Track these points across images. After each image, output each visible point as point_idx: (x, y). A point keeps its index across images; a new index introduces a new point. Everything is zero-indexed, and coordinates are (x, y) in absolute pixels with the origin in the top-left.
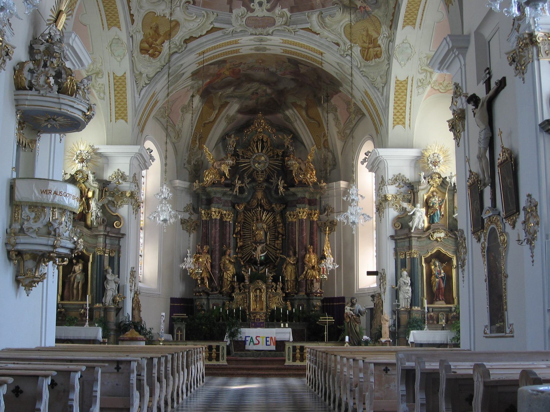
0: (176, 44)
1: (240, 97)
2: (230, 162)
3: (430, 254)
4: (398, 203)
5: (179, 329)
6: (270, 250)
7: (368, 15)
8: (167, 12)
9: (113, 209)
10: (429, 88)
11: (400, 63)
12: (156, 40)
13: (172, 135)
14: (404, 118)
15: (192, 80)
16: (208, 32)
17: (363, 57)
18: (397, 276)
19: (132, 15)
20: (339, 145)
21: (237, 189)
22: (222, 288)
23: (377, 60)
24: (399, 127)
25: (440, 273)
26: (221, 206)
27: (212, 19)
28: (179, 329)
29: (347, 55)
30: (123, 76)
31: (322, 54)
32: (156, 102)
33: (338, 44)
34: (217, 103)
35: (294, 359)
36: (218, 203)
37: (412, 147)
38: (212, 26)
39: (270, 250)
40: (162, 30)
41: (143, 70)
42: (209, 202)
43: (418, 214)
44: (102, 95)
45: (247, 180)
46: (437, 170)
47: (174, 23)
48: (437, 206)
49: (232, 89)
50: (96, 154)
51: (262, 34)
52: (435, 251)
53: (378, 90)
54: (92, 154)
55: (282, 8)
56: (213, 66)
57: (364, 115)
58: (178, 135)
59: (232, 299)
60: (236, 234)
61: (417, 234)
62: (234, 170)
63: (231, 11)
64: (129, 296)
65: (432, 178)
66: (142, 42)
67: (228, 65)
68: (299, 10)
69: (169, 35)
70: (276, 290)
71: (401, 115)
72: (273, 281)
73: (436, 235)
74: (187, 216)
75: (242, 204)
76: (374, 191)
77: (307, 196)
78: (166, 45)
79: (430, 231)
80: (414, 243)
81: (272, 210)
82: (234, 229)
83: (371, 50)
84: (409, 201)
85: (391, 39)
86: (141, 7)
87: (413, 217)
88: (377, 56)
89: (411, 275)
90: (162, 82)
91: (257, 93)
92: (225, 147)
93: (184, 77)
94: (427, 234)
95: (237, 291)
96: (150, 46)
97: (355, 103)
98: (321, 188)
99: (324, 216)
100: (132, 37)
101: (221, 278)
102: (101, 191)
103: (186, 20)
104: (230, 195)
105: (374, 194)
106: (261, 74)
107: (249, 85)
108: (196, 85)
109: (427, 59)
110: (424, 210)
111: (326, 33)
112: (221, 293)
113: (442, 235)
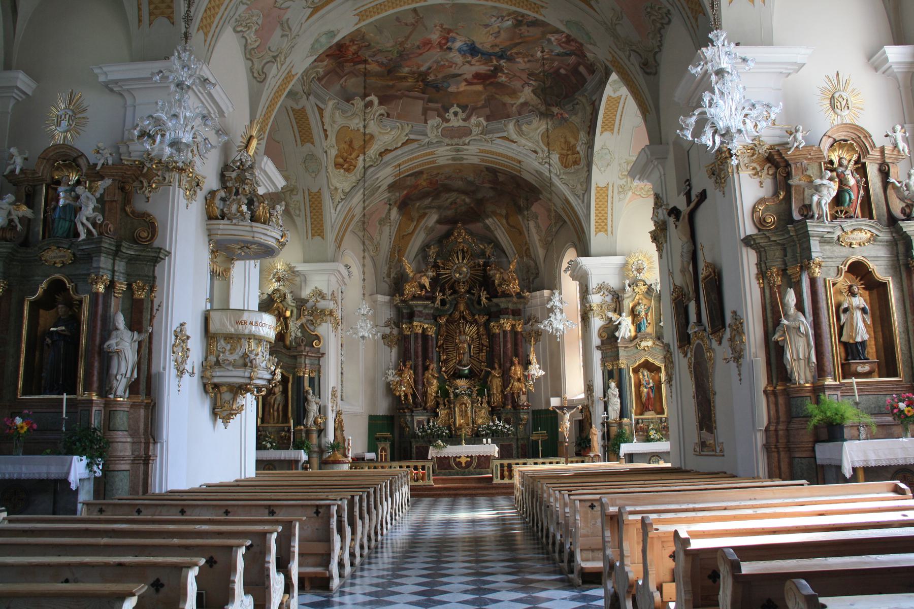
0: (371, 158)
1: (439, 208)
2: (431, 274)
3: (637, 364)
4: (603, 312)
5: (383, 449)
6: (475, 363)
7: (566, 121)
8: (361, 125)
9: (312, 328)
10: (630, 193)
11: (600, 170)
12: (351, 154)
13: (371, 248)
14: (606, 225)
15: (389, 192)
16: (403, 144)
17: (562, 164)
18: (606, 387)
19: (325, 131)
20: (541, 252)
21: (438, 302)
22: (426, 404)
23: (576, 167)
24: (601, 235)
25: (649, 383)
26: (422, 319)
27: (407, 131)
28: (383, 449)
29: (546, 162)
30: (318, 192)
31: (520, 162)
32: (353, 217)
33: (536, 152)
34: (415, 215)
35: (502, 477)
36: (419, 316)
37: (614, 254)
38: (407, 138)
39: (475, 363)
40: (357, 144)
41: (338, 185)
42: (411, 317)
43: (624, 324)
44: (297, 212)
45: (448, 292)
46: (641, 276)
47: (367, 137)
48: (643, 314)
49: (430, 199)
50: (293, 272)
51: (458, 145)
52: (642, 360)
53: (579, 197)
54: (289, 272)
55: (478, 118)
56: (409, 178)
57: (565, 222)
58: (377, 248)
59: (437, 415)
60: (439, 347)
61: (624, 344)
62: (434, 281)
63: (426, 122)
64: (331, 417)
65: (637, 286)
66: (336, 157)
67: (425, 176)
68: (495, 119)
69: (363, 150)
70: (481, 404)
71: (603, 222)
72: (478, 395)
73: (643, 344)
74: (387, 330)
75: (444, 316)
76: (579, 300)
77: (511, 306)
78: (361, 158)
79: (637, 340)
80: (622, 353)
81: (475, 322)
82: (437, 343)
83: (570, 156)
84: (615, 311)
85: (590, 145)
86: (334, 122)
87: (620, 326)
88: (576, 163)
89: (620, 386)
90: (358, 197)
91: (456, 203)
92: (425, 257)
93: (380, 190)
94: (634, 343)
95: (442, 407)
96: (345, 161)
97: (555, 210)
98: (524, 298)
99: (528, 326)
100: (326, 152)
101: (425, 394)
102: (299, 309)
103: (380, 133)
104: (432, 308)
105: (579, 302)
106: (459, 184)
107: (447, 195)
108: (393, 197)
109: (628, 164)
110: (629, 319)
111: (523, 141)
112: (425, 409)
113: (650, 343)
